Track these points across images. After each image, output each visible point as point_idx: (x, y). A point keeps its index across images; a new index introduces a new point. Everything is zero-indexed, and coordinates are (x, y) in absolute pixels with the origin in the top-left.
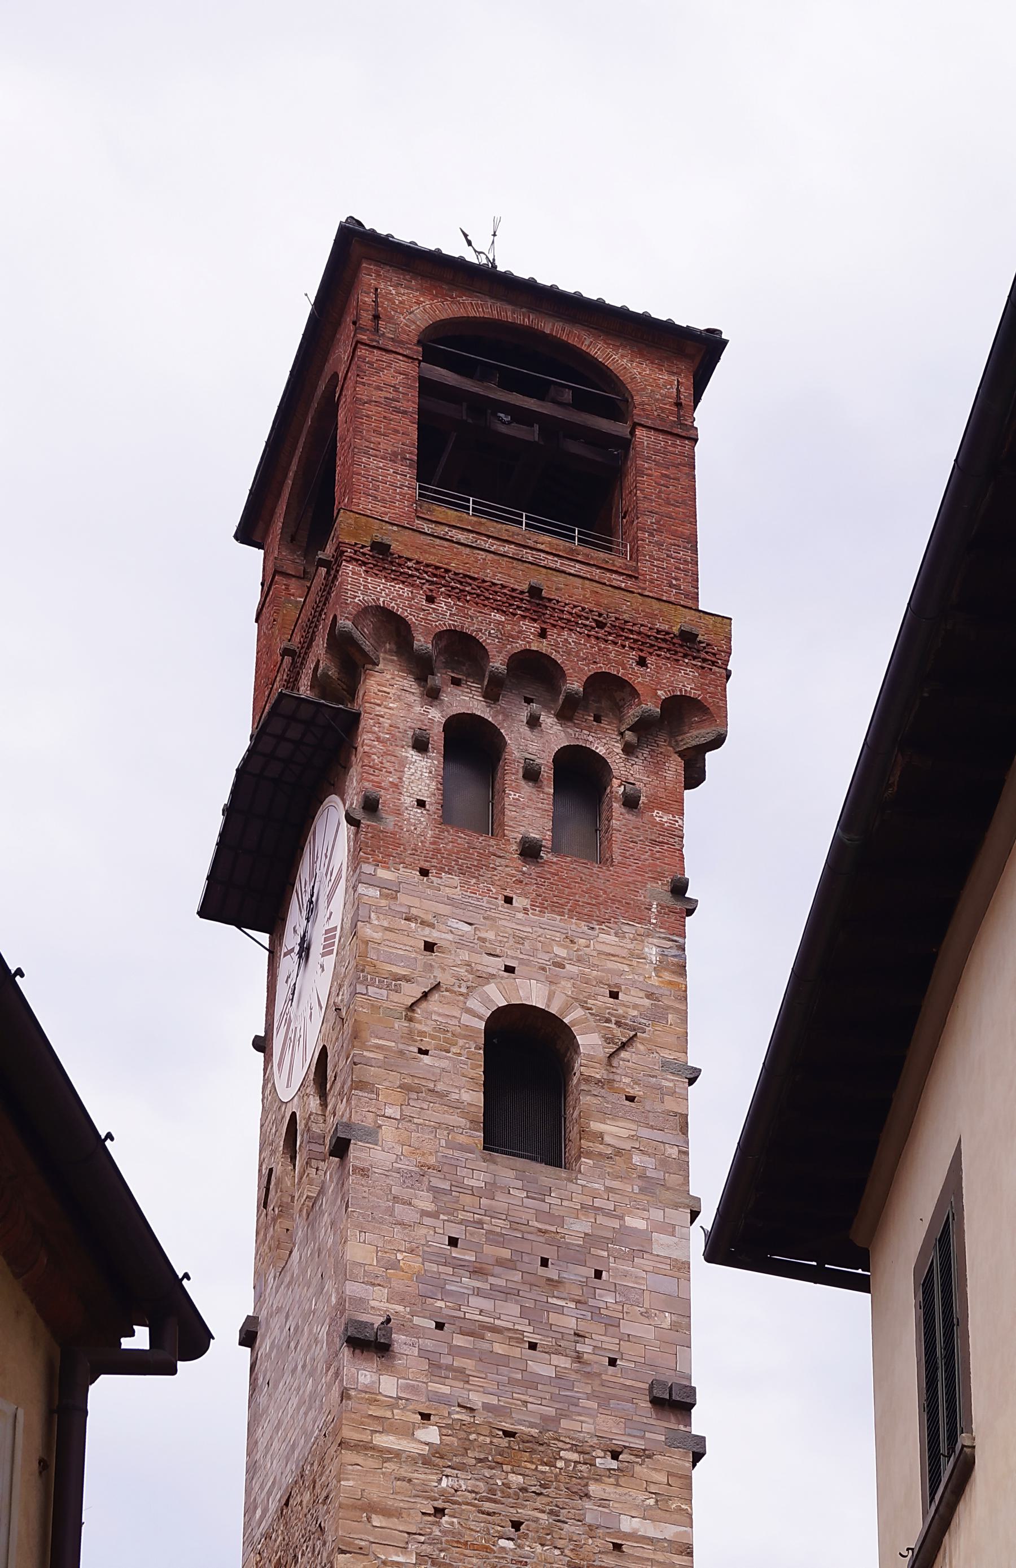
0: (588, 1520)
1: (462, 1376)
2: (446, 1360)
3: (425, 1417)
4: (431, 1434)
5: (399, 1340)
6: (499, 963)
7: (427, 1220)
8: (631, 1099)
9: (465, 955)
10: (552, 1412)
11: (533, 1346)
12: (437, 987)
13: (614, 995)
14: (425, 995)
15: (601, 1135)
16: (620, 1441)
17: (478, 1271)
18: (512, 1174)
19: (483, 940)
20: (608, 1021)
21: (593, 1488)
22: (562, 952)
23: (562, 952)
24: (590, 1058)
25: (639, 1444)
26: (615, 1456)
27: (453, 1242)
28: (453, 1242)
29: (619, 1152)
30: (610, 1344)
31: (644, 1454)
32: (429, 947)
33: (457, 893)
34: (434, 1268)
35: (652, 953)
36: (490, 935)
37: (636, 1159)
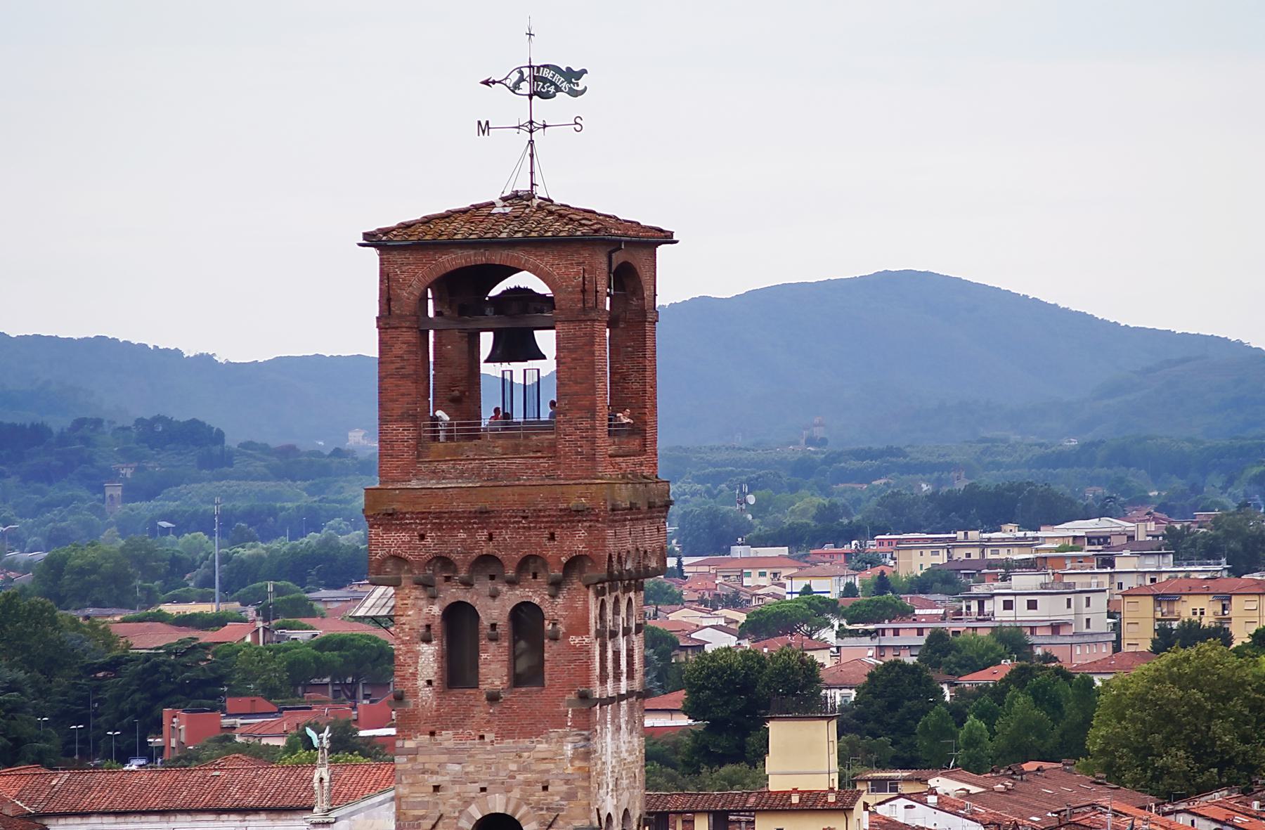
6: (477, 786)
9: (457, 788)
19: (467, 773)
20: (542, 809)
23: (513, 767)
33: (449, 744)
35: (568, 749)
36: (471, 769)
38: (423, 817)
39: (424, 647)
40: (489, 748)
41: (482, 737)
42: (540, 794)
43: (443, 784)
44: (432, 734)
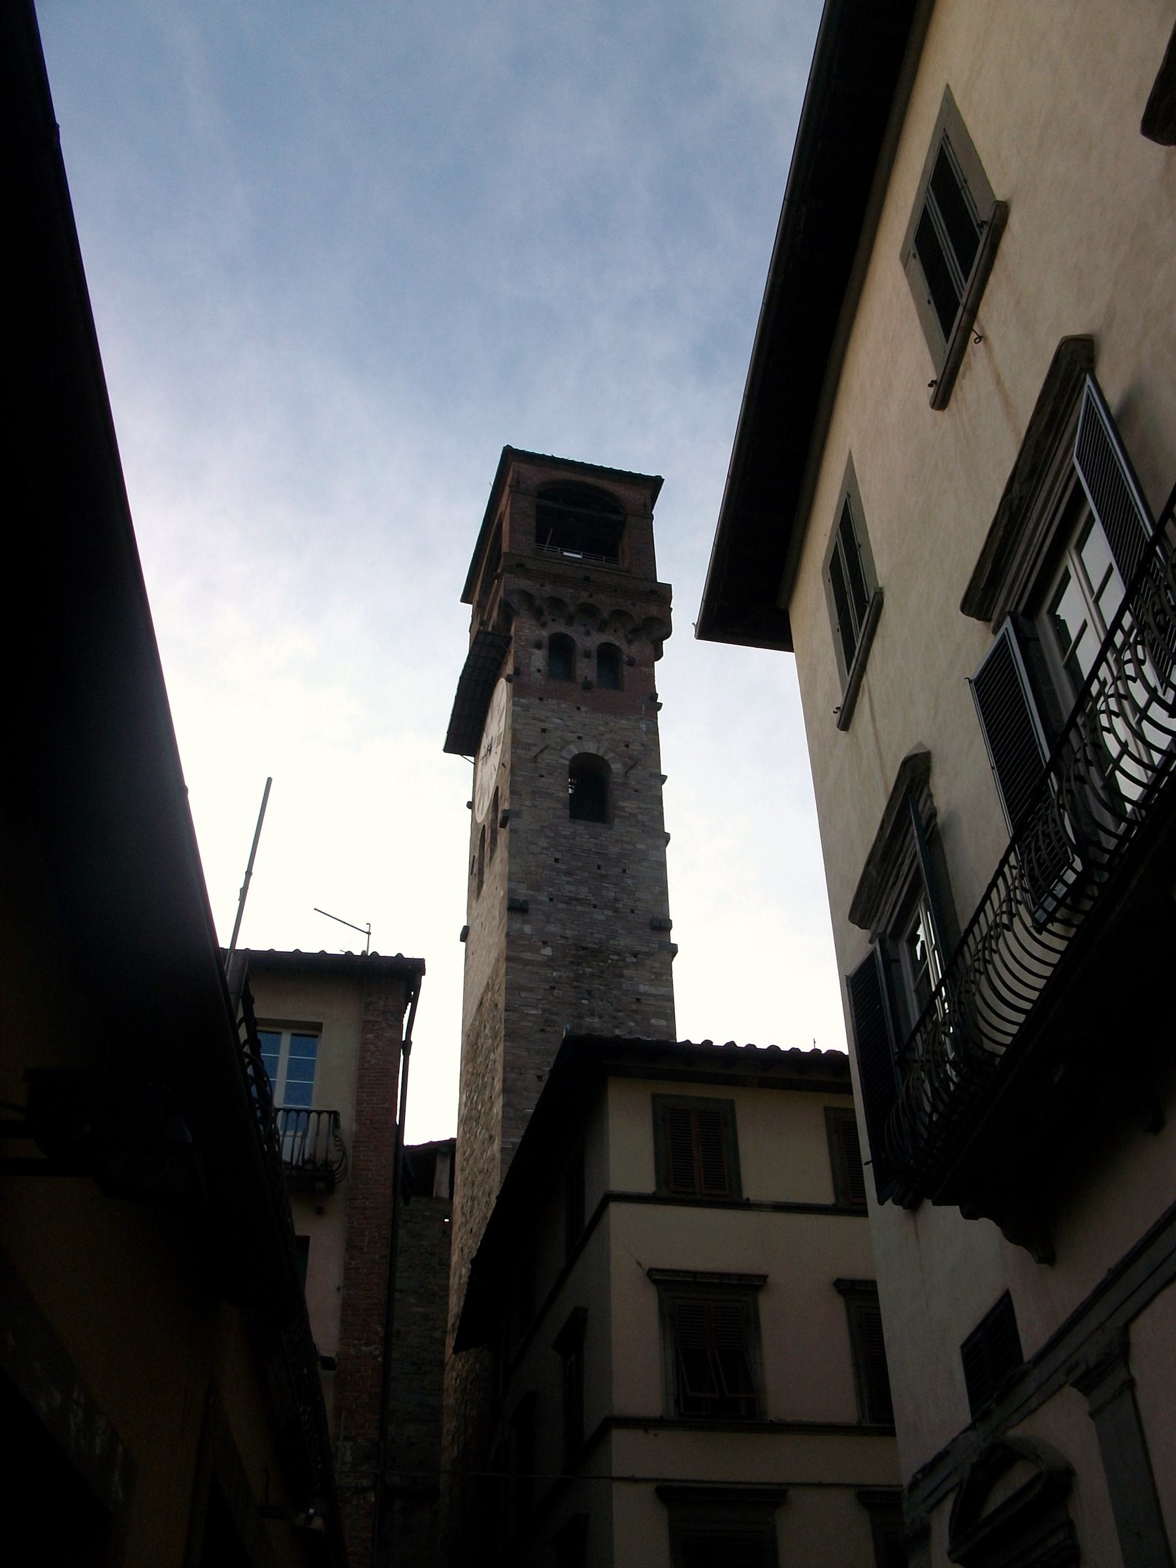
4: (548, 951)
5: (531, 906)
6: (576, 735)
8: (636, 791)
12: (547, 747)
13: (627, 746)
14: (542, 751)
16: (638, 948)
17: (568, 873)
21: (625, 972)
22: (603, 729)
23: (603, 729)
25: (647, 949)
26: (635, 956)
27: (557, 860)
28: (557, 860)
29: (632, 815)
31: (649, 954)
32: (544, 730)
35: (643, 726)
36: (571, 724)
37: (640, 817)
38: (534, 745)
39: (536, 651)
41: (578, 709)
42: (623, 748)
44: (541, 699)
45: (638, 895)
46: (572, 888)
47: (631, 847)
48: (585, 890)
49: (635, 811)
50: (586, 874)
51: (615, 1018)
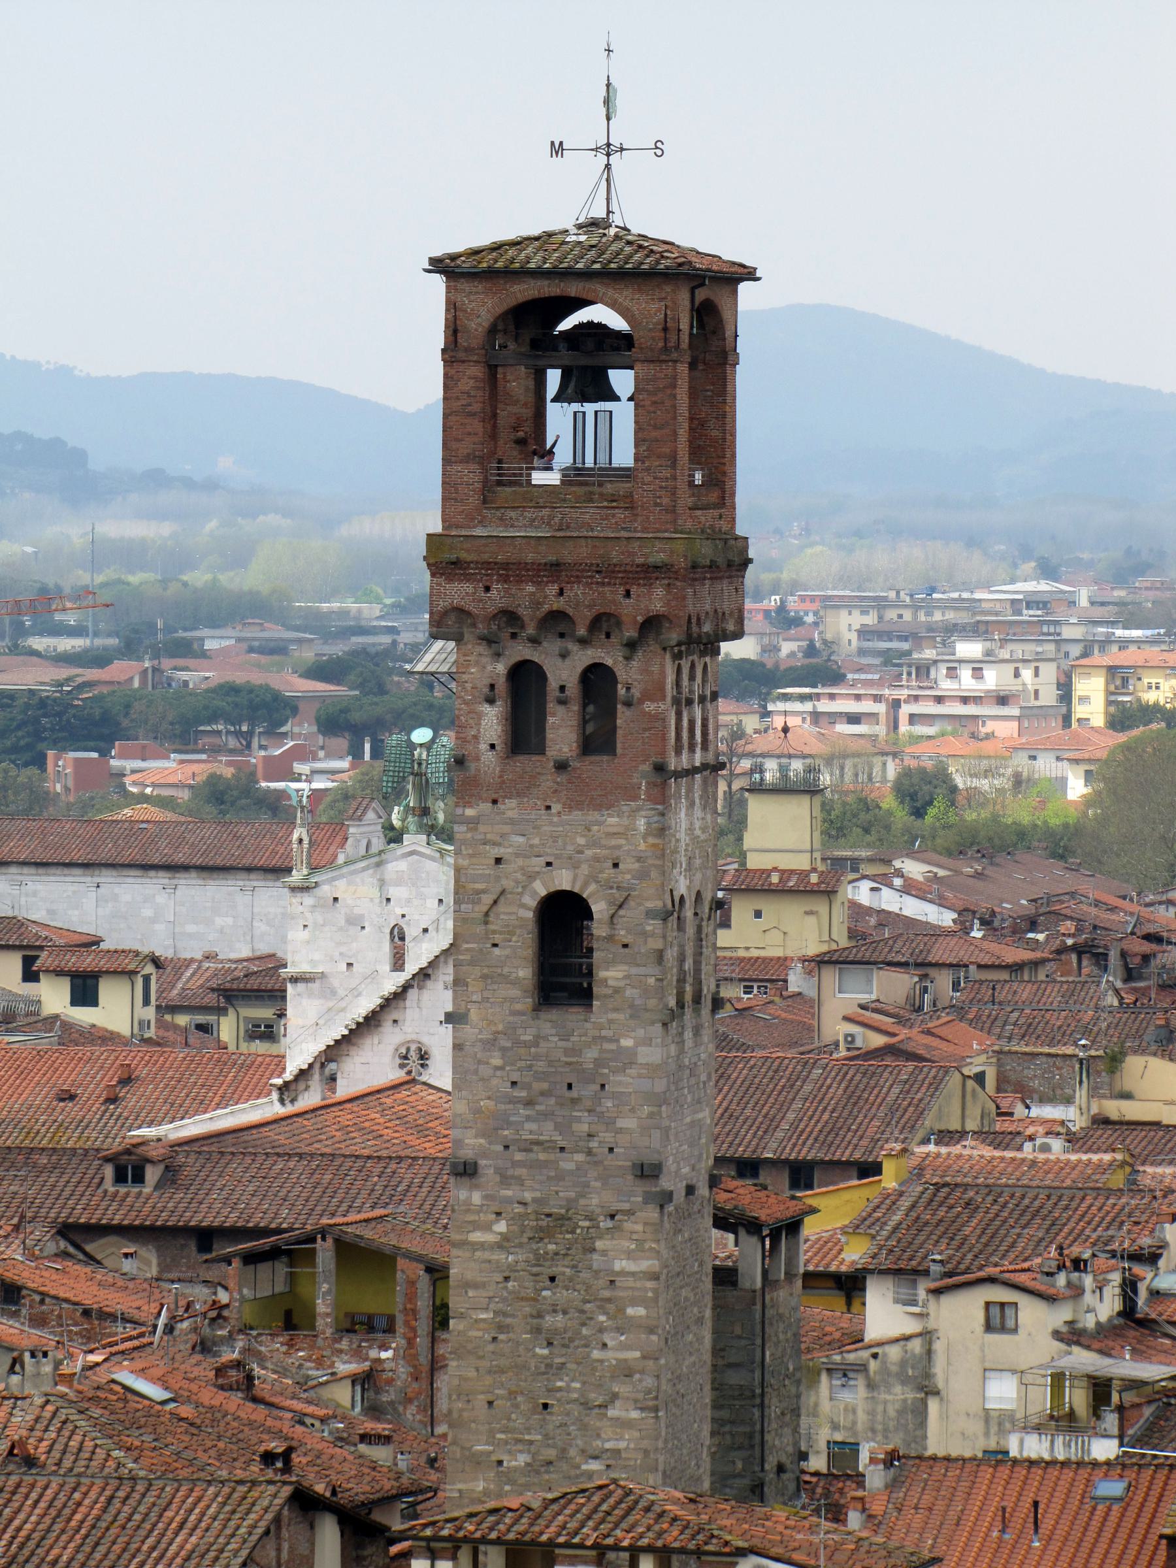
0: (595, 1267)
1: (520, 1181)
2: (510, 1172)
3: (498, 1214)
4: (501, 1227)
5: (482, 1162)
6: (541, 861)
7: (498, 1073)
8: (625, 946)
9: (520, 862)
10: (573, 1195)
11: (562, 1149)
12: (503, 892)
15: (606, 980)
17: (529, 1103)
18: (549, 1025)
19: (531, 846)
21: (599, 1244)
22: (581, 841)
23: (581, 841)
24: (600, 921)
25: (626, 1206)
26: (612, 1217)
27: (514, 1083)
29: (617, 990)
30: (608, 1137)
31: (630, 1213)
32: (498, 861)
34: (503, 1107)
36: (536, 841)
37: (629, 992)
40: (555, 819)
41: (548, 808)
43: (506, 857)
44: (495, 802)
45: (621, 1123)
46: (533, 1126)
47: (613, 1046)
48: (549, 1126)
49: (621, 984)
50: (552, 1101)
51: (582, 1312)
